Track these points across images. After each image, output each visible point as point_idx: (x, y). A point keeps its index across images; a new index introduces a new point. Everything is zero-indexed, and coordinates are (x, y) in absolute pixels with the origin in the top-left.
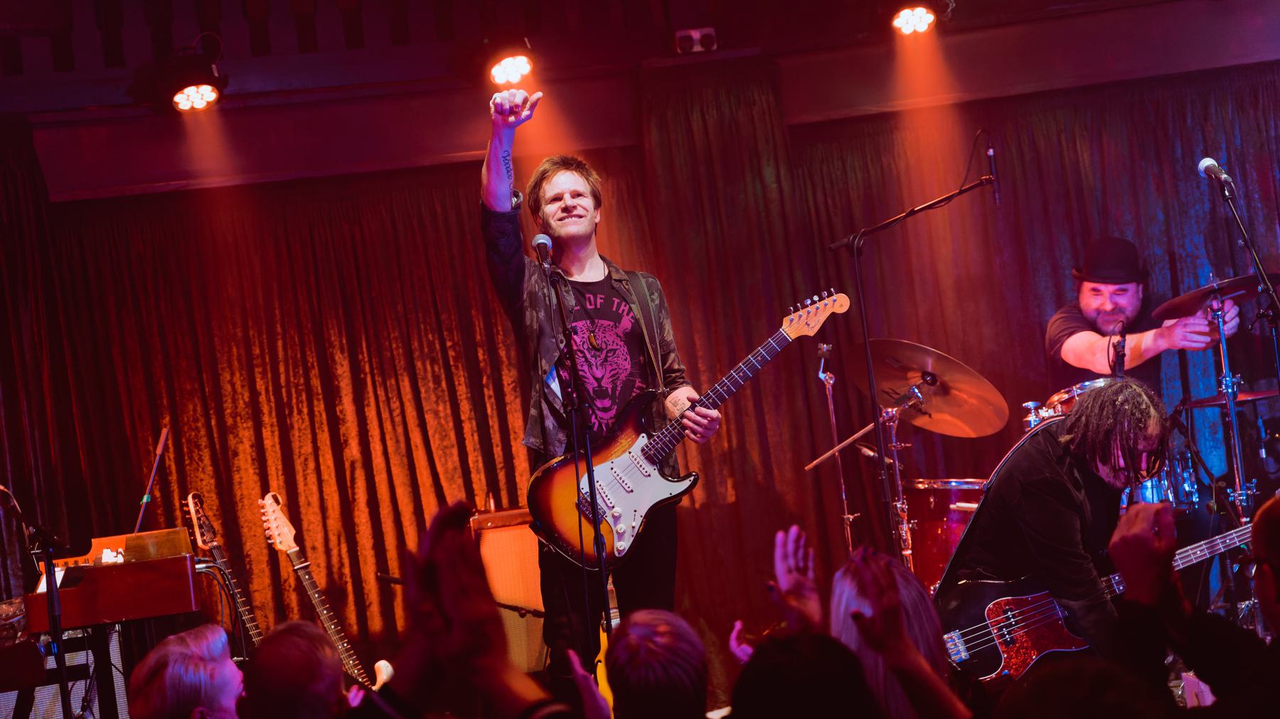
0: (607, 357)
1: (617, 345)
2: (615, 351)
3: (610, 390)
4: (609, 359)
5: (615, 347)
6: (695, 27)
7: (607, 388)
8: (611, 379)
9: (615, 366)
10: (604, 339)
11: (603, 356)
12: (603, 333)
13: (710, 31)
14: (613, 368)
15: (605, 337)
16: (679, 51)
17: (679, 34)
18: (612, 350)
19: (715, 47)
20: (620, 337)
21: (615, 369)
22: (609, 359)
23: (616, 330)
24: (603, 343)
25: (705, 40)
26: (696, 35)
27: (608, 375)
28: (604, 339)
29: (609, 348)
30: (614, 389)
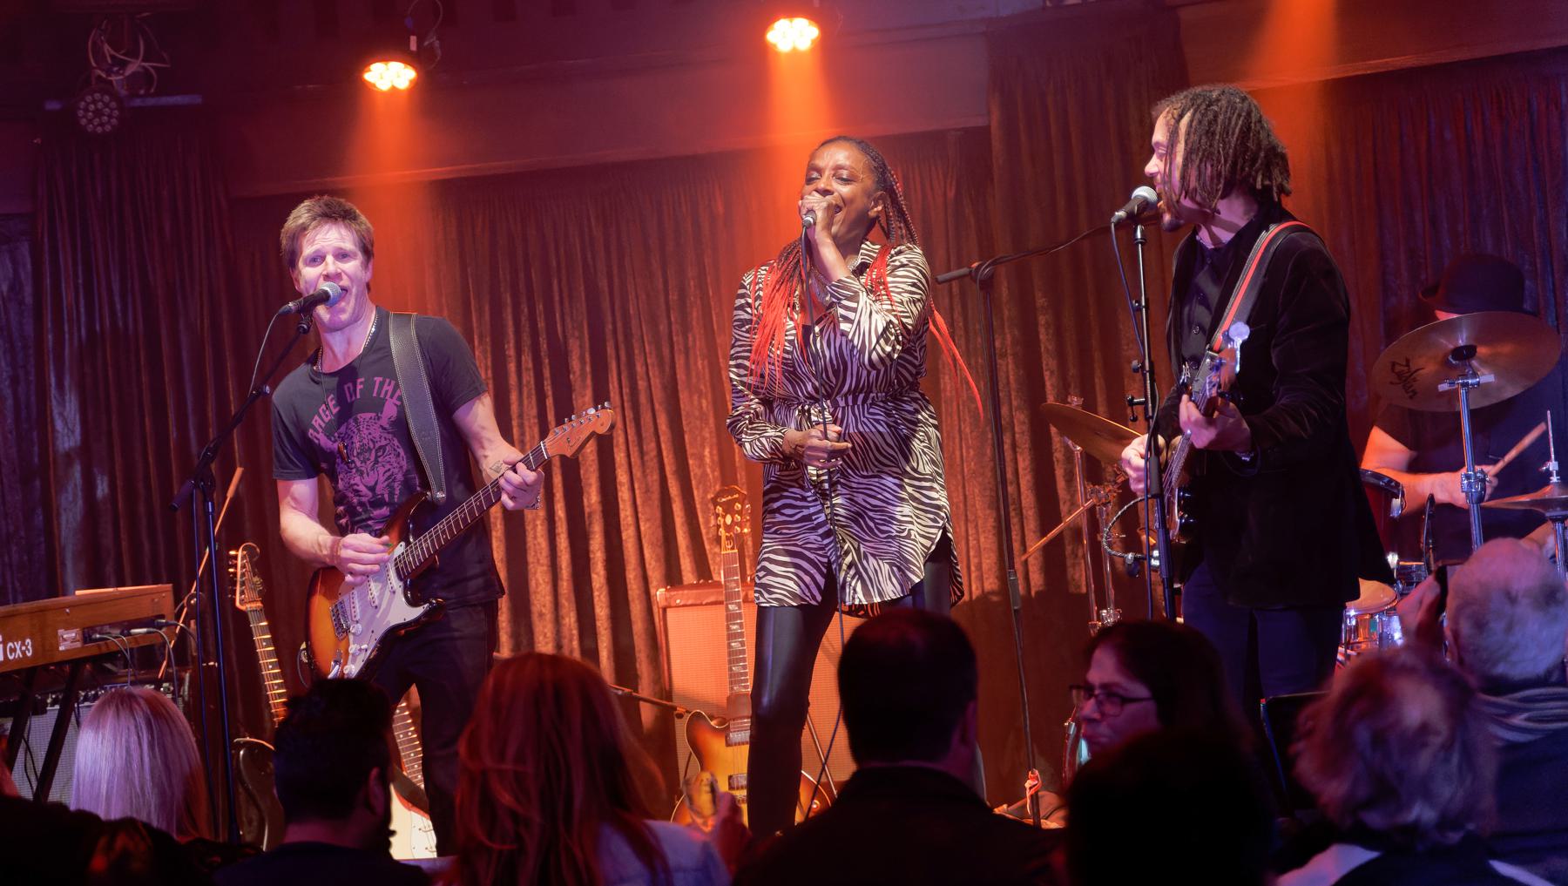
0: (377, 457)
1: (386, 439)
2: (383, 448)
3: (386, 496)
4: (380, 460)
5: (384, 442)
7: (383, 495)
8: (386, 483)
9: (388, 467)
10: (370, 437)
11: (372, 459)
12: (367, 429)
14: (387, 469)
15: (370, 434)
18: (380, 447)
20: (385, 429)
21: (389, 470)
22: (380, 460)
23: (380, 422)
24: (370, 442)
27: (382, 479)
28: (370, 437)
29: (377, 446)
30: (391, 494)
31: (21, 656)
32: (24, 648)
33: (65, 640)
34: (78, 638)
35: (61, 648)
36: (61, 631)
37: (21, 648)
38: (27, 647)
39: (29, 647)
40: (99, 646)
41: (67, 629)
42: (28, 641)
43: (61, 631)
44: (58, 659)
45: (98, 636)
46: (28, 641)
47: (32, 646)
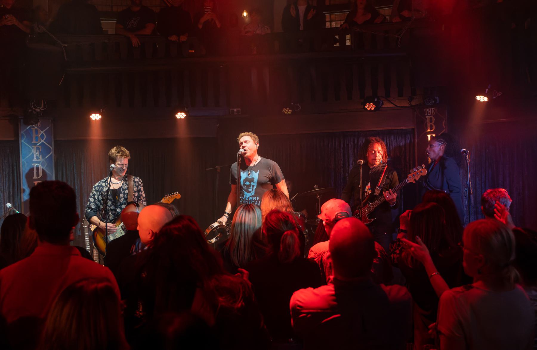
6: (235, 108)
13: (240, 109)
16: (231, 114)
17: (231, 109)
19: (240, 114)
25: (238, 111)
26: (235, 110)
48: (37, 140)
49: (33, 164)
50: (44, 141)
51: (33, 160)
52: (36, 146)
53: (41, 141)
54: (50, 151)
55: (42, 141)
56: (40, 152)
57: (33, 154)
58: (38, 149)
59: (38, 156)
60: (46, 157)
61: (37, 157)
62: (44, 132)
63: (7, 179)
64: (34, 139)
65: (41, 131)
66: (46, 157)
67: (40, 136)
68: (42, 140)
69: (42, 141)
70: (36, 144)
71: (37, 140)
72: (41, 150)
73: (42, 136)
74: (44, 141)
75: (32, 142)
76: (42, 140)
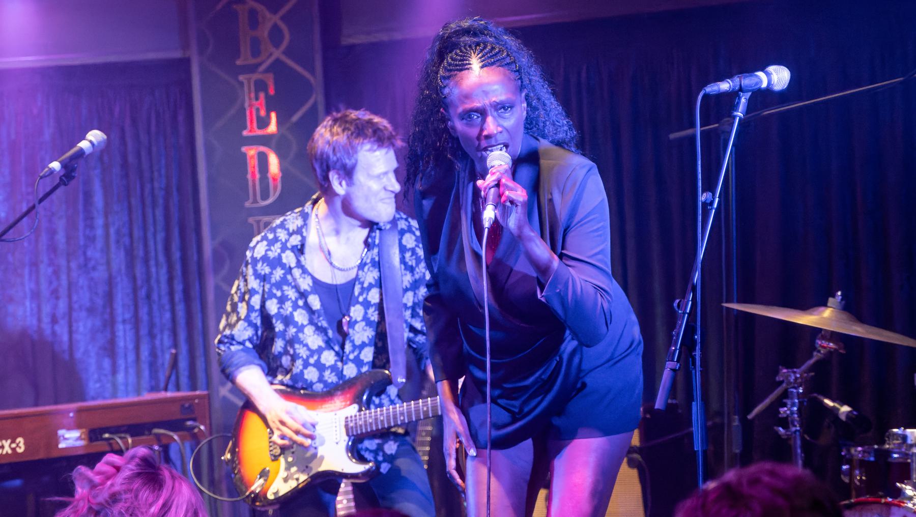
31: (10, 452)
32: (14, 445)
33: (66, 439)
34: (83, 436)
35: (62, 445)
36: (61, 432)
37: (10, 446)
38: (18, 445)
39: (22, 445)
40: (110, 445)
41: (69, 429)
42: (20, 440)
43: (61, 432)
44: (55, 454)
45: (107, 435)
46: (20, 440)
47: (25, 444)
48: (256, 52)
49: (243, 149)
50: (284, 53)
51: (245, 133)
52: (255, 76)
53: (271, 55)
54: (306, 89)
55: (277, 54)
56: (267, 97)
57: (242, 110)
58: (260, 86)
59: (263, 113)
60: (295, 118)
61: (259, 119)
62: (283, 19)
63: (159, 213)
64: (242, 49)
65: (268, 15)
66: (295, 118)
67: (266, 34)
68: (277, 45)
69: (277, 54)
70: (252, 69)
71: (256, 52)
72: (272, 92)
73: (276, 36)
74: (284, 53)
75: (238, 62)
76: (273, 49)
